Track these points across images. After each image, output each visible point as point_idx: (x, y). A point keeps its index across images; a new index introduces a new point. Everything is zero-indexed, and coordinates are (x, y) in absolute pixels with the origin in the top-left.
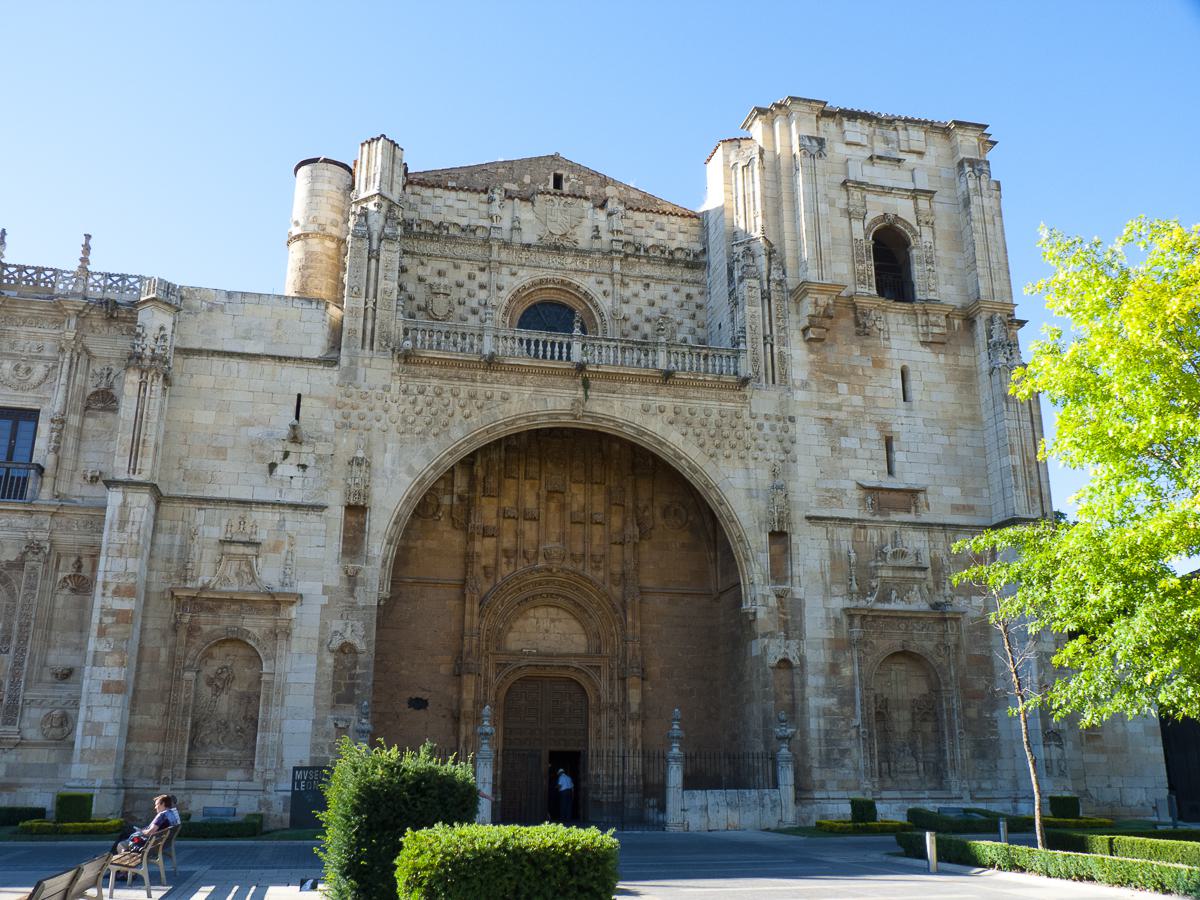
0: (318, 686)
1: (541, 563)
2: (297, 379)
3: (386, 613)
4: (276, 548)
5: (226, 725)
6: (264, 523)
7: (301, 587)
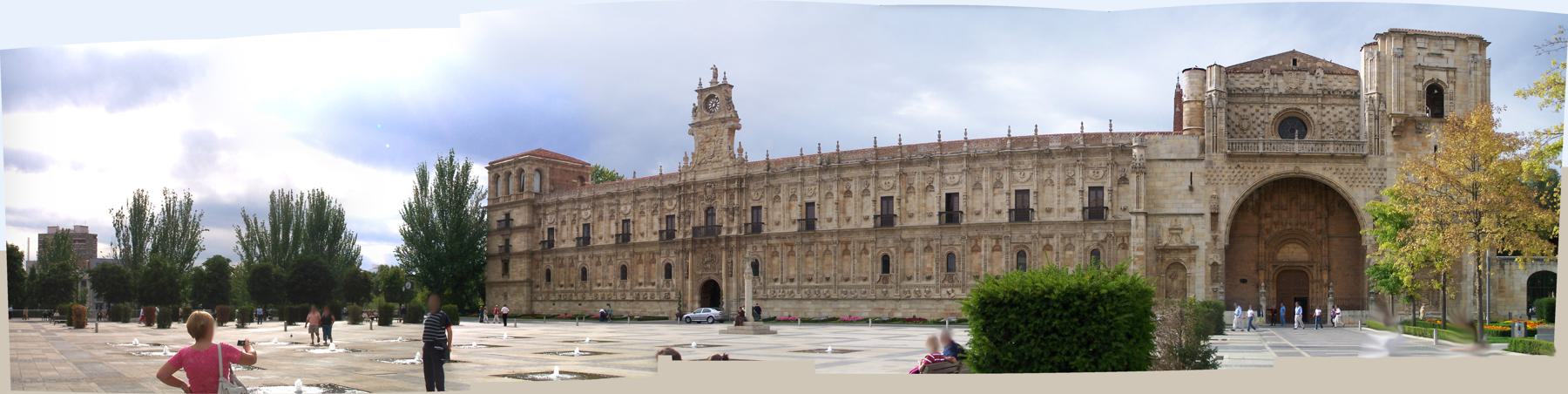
0: (1206, 277)
1: (1288, 227)
2: (1189, 167)
3: (1228, 251)
4: (1188, 230)
5: (1176, 291)
6: (1184, 222)
7: (1198, 243)
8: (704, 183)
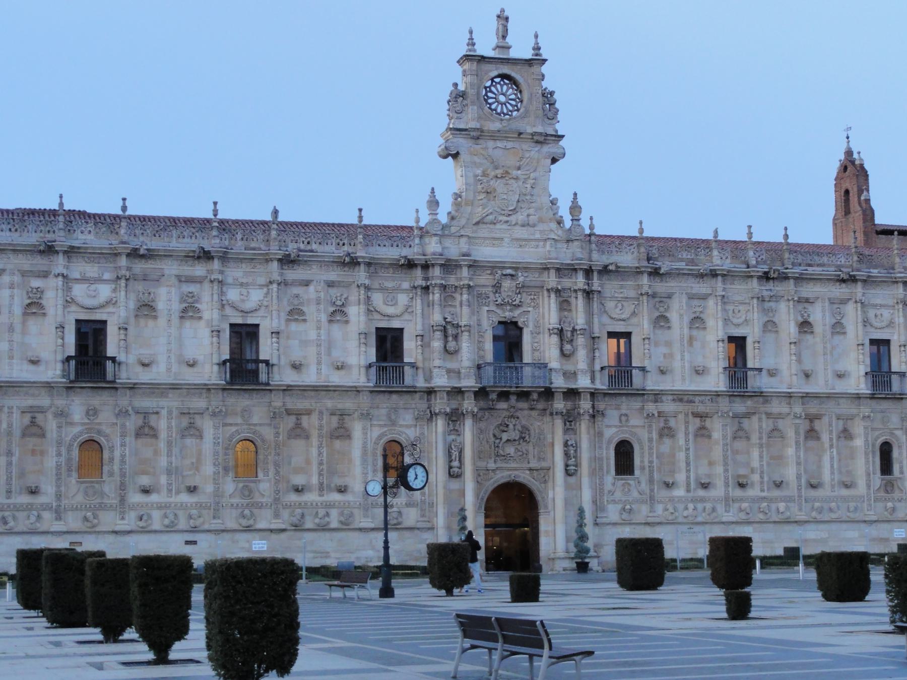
8: (494, 267)
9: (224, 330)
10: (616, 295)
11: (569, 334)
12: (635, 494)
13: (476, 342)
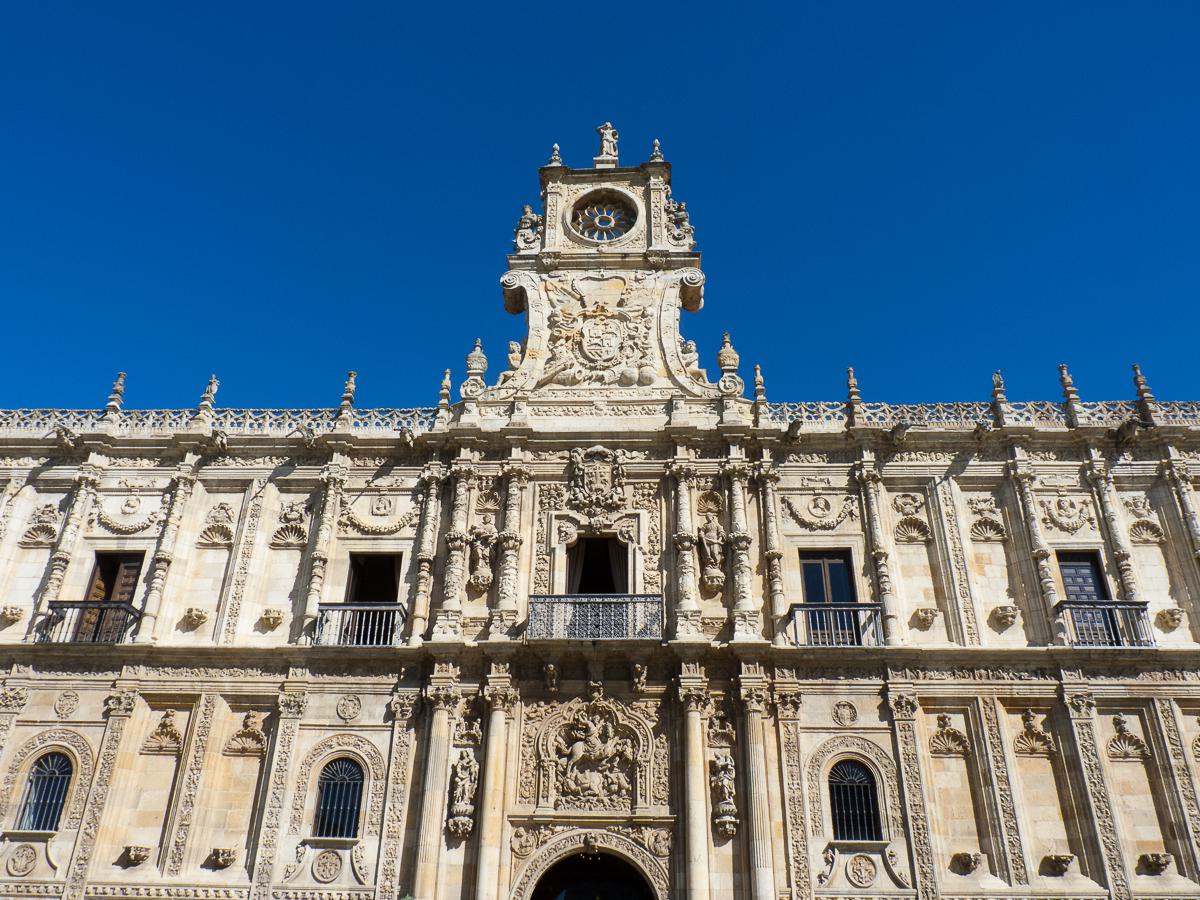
9: (81, 562)
10: (812, 485)
11: (717, 549)
12: (883, 883)
13: (533, 571)
